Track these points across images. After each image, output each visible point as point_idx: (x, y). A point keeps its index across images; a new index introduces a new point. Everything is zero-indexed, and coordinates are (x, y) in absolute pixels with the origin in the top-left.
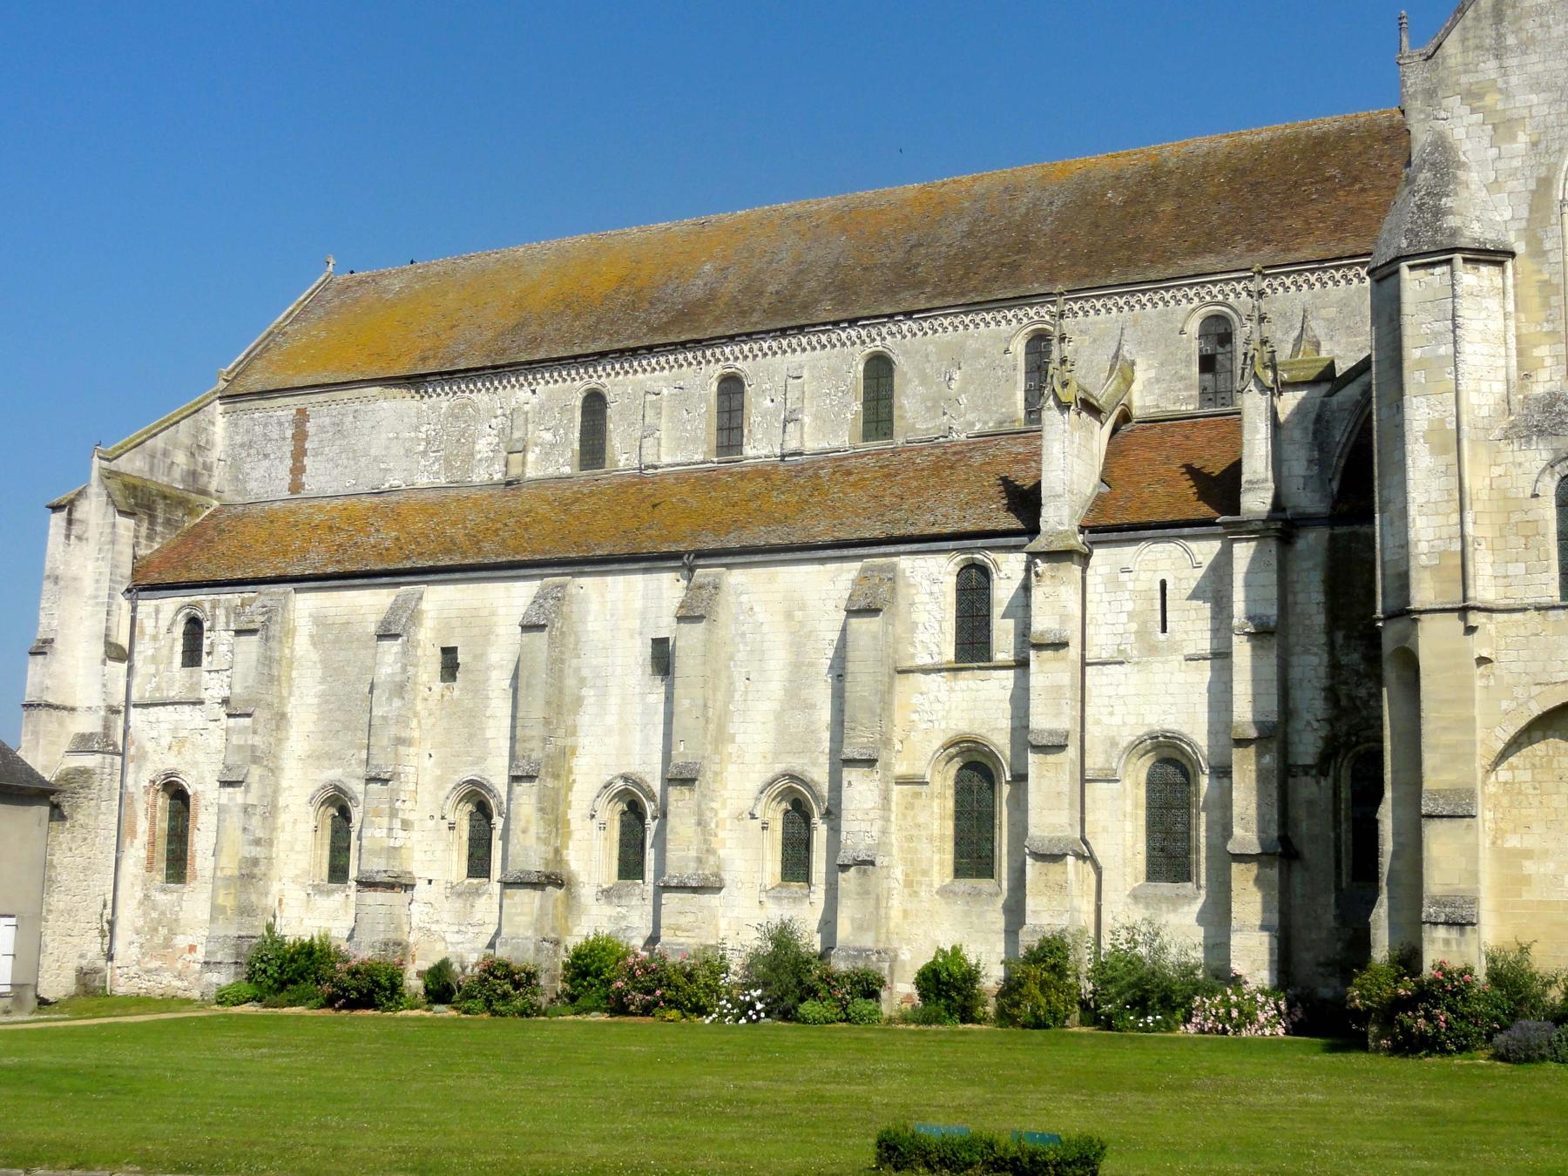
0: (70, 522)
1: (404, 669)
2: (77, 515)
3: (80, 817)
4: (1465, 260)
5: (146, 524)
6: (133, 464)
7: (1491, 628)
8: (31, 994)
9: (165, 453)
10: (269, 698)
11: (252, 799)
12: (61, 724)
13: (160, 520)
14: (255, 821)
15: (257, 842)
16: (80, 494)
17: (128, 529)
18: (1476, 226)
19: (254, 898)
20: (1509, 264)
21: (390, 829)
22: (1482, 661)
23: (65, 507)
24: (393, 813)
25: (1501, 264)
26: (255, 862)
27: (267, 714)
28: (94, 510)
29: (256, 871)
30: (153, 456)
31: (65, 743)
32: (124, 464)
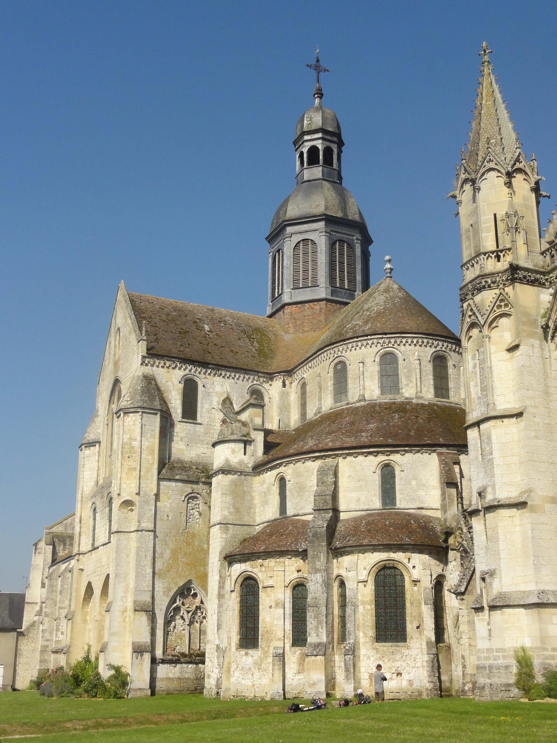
0: (36, 549)
1: (62, 586)
2: (38, 547)
3: (31, 635)
4: (85, 447)
5: (62, 546)
6: (59, 529)
7: (84, 559)
8: (9, 688)
9: (71, 524)
10: (52, 597)
11: (45, 627)
12: (33, 608)
13: (68, 544)
14: (47, 634)
15: (48, 640)
16: (40, 541)
17: (50, 549)
18: (91, 435)
19: (46, 657)
20: (97, 445)
21: (56, 635)
22: (82, 570)
23: (36, 545)
24: (58, 630)
25: (95, 446)
26: (47, 646)
27: (51, 602)
28: (42, 544)
29: (47, 649)
30: (66, 526)
31: (34, 613)
32: (54, 530)
